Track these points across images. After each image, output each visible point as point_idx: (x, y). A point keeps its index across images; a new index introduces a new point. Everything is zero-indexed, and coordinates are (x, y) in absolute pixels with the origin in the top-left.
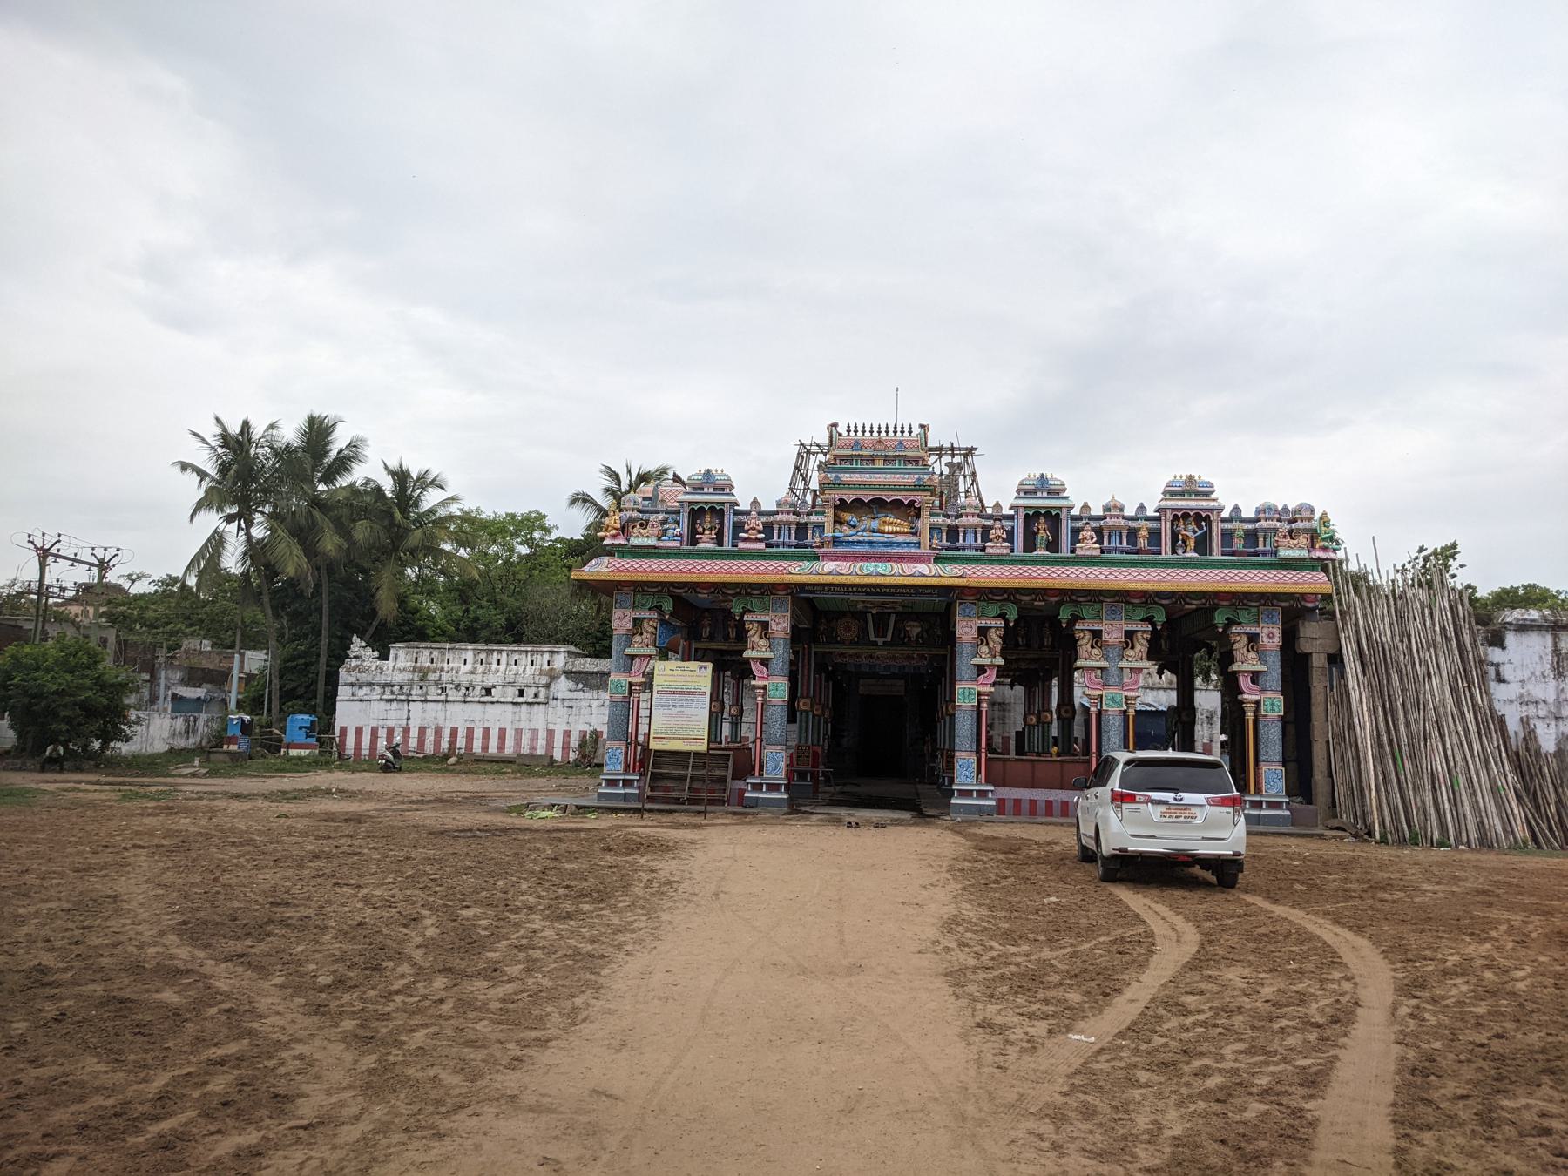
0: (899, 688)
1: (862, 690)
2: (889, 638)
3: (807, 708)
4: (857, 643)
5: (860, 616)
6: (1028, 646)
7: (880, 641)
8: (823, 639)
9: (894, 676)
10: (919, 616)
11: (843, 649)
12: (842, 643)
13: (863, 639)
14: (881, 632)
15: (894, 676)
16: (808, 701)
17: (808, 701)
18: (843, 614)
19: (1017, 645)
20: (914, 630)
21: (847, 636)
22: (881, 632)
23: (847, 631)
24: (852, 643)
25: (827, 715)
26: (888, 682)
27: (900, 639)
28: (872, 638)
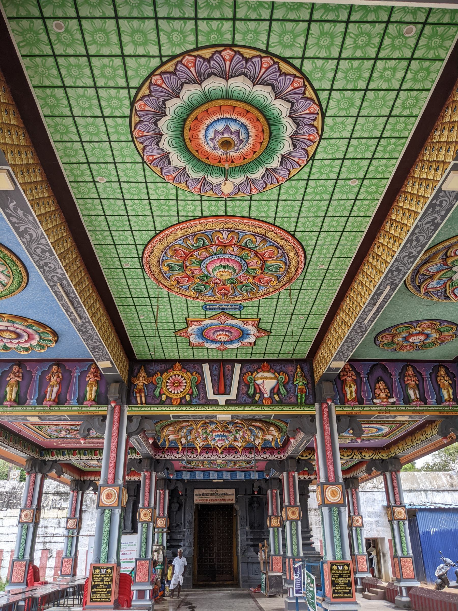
0: (229, 496)
1: (197, 500)
2: (233, 395)
3: (113, 501)
4: (189, 403)
5: (191, 365)
6: (423, 400)
7: (222, 399)
8: (140, 398)
9: (226, 484)
10: (273, 364)
11: (171, 412)
12: (169, 402)
13: (197, 396)
14: (222, 386)
15: (226, 484)
16: (114, 491)
17: (114, 491)
18: (168, 364)
19: (407, 401)
20: (267, 382)
21: (177, 393)
22: (222, 386)
23: (175, 385)
24: (182, 402)
25: (161, 523)
26: (220, 491)
27: (250, 396)
28: (211, 395)
